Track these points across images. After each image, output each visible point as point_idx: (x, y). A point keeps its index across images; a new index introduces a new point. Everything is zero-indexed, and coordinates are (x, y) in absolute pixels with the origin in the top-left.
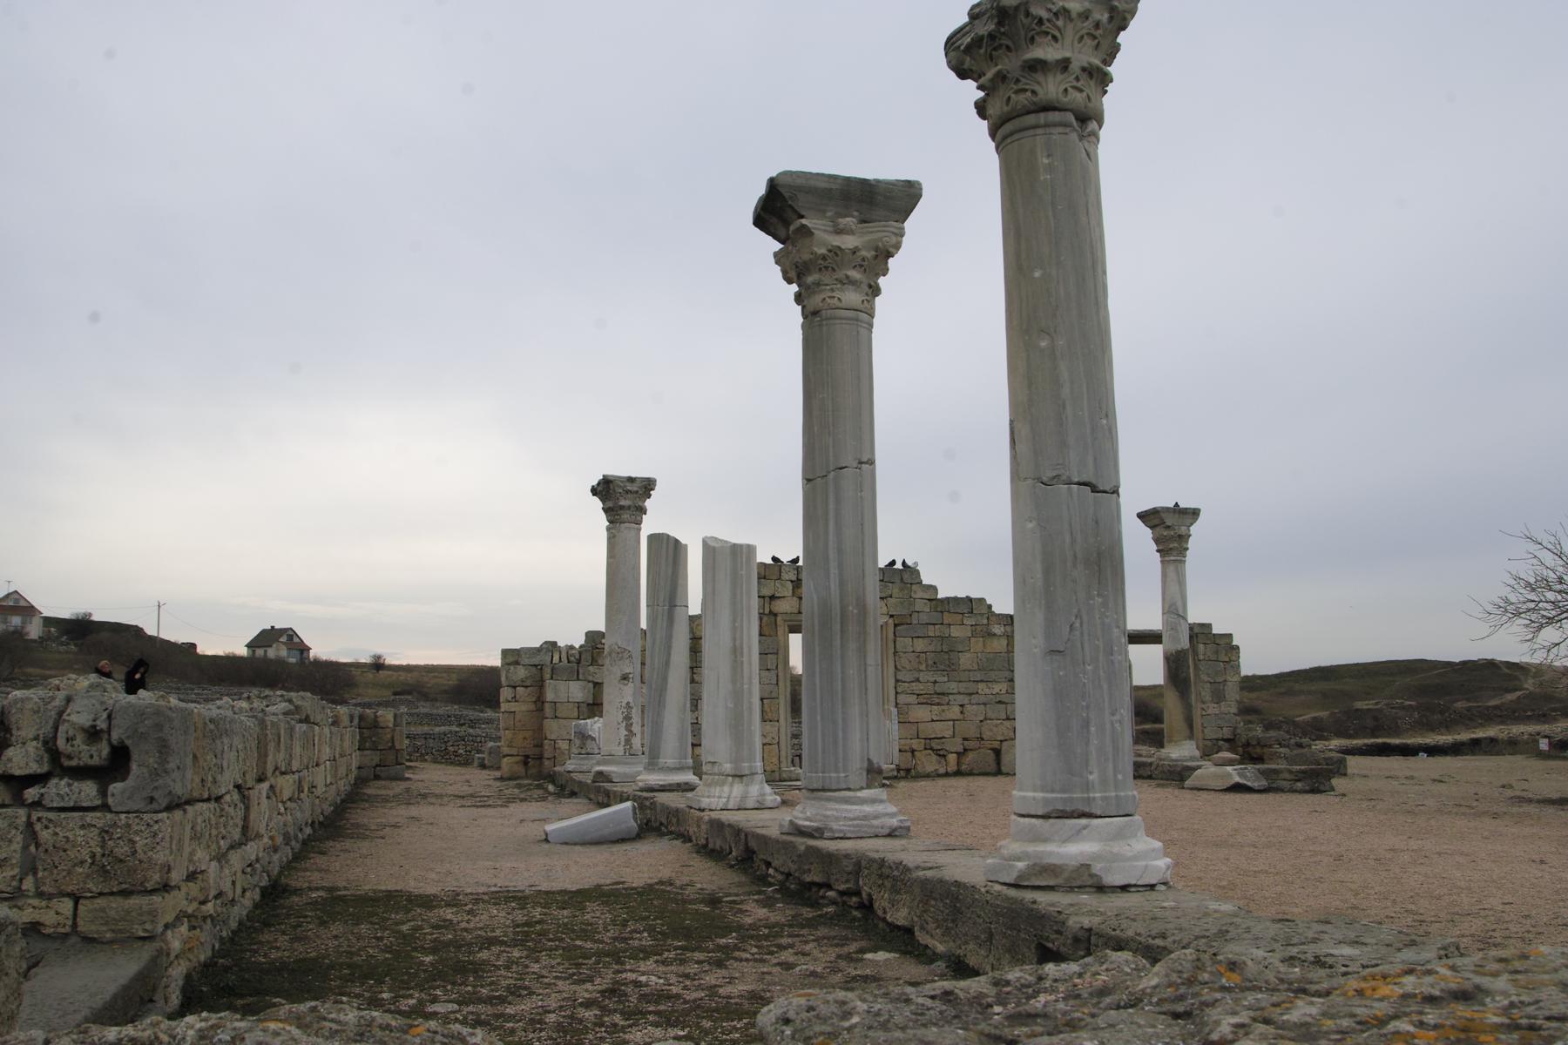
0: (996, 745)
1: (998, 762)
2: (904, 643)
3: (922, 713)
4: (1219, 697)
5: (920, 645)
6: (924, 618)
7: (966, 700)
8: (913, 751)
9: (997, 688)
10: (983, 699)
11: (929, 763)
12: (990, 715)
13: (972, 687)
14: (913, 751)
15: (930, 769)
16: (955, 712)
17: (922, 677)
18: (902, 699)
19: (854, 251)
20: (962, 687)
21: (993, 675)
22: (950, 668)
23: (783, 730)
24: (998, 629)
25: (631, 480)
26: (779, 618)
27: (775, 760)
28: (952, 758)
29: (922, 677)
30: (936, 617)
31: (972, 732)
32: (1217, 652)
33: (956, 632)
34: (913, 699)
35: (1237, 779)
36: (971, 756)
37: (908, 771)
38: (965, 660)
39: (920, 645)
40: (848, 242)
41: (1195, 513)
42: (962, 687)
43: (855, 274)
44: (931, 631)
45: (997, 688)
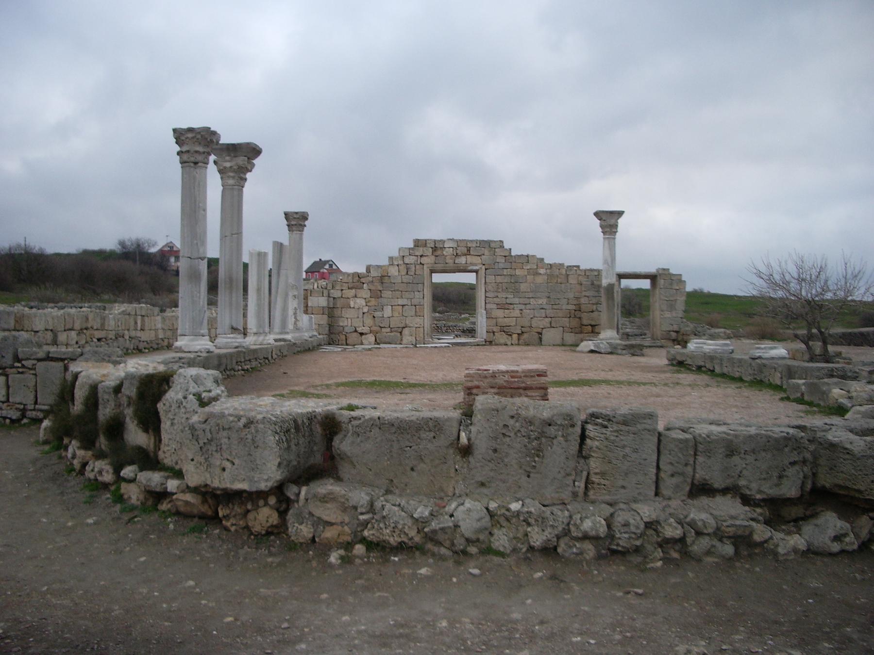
0: (539, 330)
1: (541, 339)
2: (490, 278)
3: (500, 313)
4: (672, 307)
5: (499, 279)
6: (501, 266)
7: (523, 307)
8: (494, 332)
9: (540, 302)
10: (532, 307)
11: (502, 338)
12: (537, 315)
13: (527, 301)
14: (494, 332)
15: (502, 341)
16: (517, 313)
17: (500, 295)
18: (488, 306)
19: (231, 167)
20: (522, 301)
21: (538, 295)
22: (516, 292)
23: (426, 321)
24: (542, 271)
25: (297, 213)
26: (425, 266)
27: (422, 335)
28: (515, 336)
29: (500, 295)
30: (508, 265)
31: (527, 324)
32: (671, 284)
33: (518, 272)
34: (495, 306)
35: (593, 348)
36: (525, 336)
37: (491, 342)
38: (523, 287)
39: (499, 279)
40: (228, 165)
41: (620, 214)
42: (522, 301)
43: (231, 174)
44: (505, 272)
45: (540, 302)
